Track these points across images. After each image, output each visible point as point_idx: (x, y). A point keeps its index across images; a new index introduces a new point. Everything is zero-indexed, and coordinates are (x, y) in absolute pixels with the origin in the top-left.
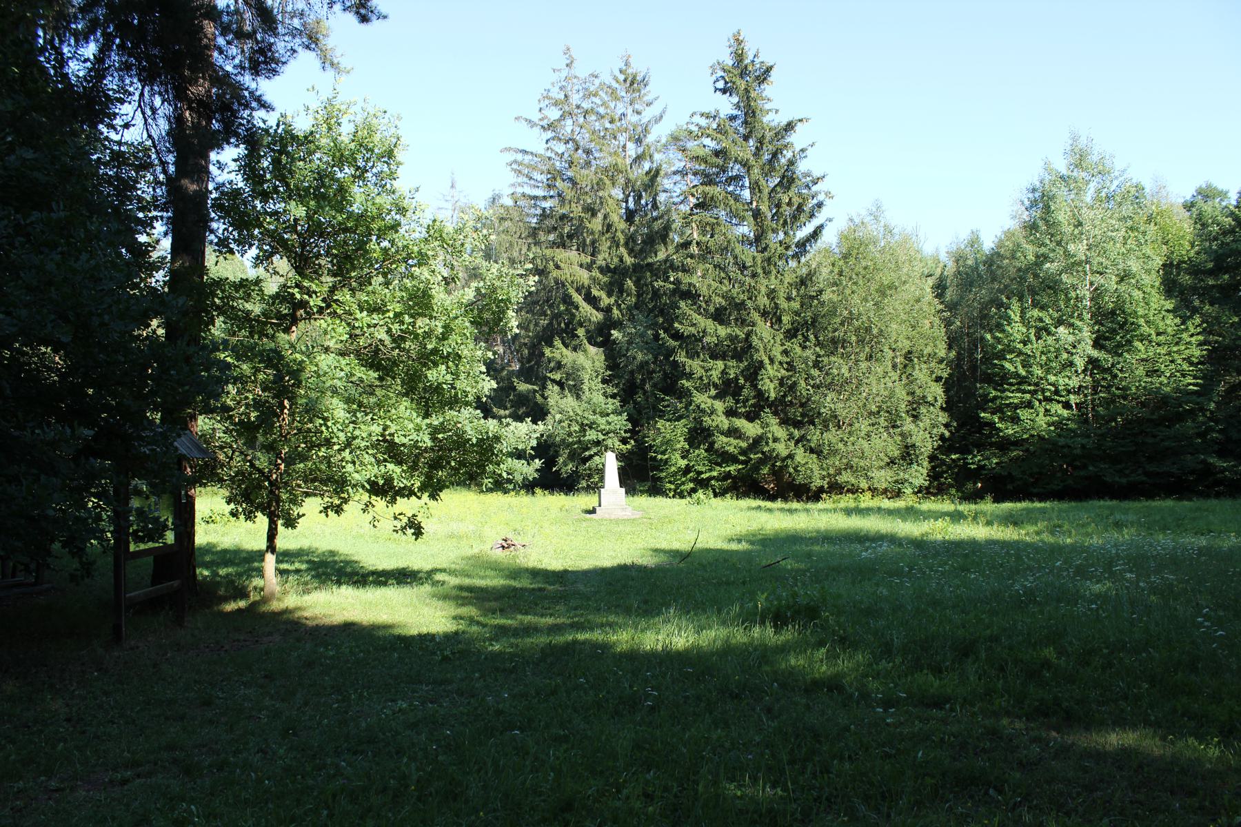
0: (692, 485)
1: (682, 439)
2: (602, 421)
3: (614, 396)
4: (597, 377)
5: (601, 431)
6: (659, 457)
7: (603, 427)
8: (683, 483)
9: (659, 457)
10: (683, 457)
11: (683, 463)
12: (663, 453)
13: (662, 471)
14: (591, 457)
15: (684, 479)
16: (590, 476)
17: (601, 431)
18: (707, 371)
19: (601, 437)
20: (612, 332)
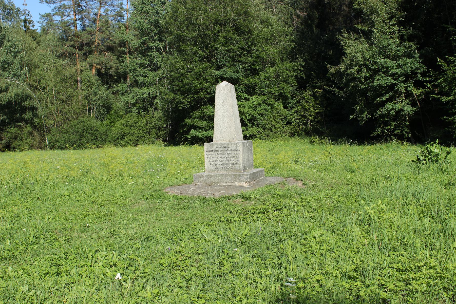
2: (390, 63)
4: (391, 18)
5: (393, 75)
7: (393, 71)
14: (383, 104)
16: (386, 124)
17: (393, 75)
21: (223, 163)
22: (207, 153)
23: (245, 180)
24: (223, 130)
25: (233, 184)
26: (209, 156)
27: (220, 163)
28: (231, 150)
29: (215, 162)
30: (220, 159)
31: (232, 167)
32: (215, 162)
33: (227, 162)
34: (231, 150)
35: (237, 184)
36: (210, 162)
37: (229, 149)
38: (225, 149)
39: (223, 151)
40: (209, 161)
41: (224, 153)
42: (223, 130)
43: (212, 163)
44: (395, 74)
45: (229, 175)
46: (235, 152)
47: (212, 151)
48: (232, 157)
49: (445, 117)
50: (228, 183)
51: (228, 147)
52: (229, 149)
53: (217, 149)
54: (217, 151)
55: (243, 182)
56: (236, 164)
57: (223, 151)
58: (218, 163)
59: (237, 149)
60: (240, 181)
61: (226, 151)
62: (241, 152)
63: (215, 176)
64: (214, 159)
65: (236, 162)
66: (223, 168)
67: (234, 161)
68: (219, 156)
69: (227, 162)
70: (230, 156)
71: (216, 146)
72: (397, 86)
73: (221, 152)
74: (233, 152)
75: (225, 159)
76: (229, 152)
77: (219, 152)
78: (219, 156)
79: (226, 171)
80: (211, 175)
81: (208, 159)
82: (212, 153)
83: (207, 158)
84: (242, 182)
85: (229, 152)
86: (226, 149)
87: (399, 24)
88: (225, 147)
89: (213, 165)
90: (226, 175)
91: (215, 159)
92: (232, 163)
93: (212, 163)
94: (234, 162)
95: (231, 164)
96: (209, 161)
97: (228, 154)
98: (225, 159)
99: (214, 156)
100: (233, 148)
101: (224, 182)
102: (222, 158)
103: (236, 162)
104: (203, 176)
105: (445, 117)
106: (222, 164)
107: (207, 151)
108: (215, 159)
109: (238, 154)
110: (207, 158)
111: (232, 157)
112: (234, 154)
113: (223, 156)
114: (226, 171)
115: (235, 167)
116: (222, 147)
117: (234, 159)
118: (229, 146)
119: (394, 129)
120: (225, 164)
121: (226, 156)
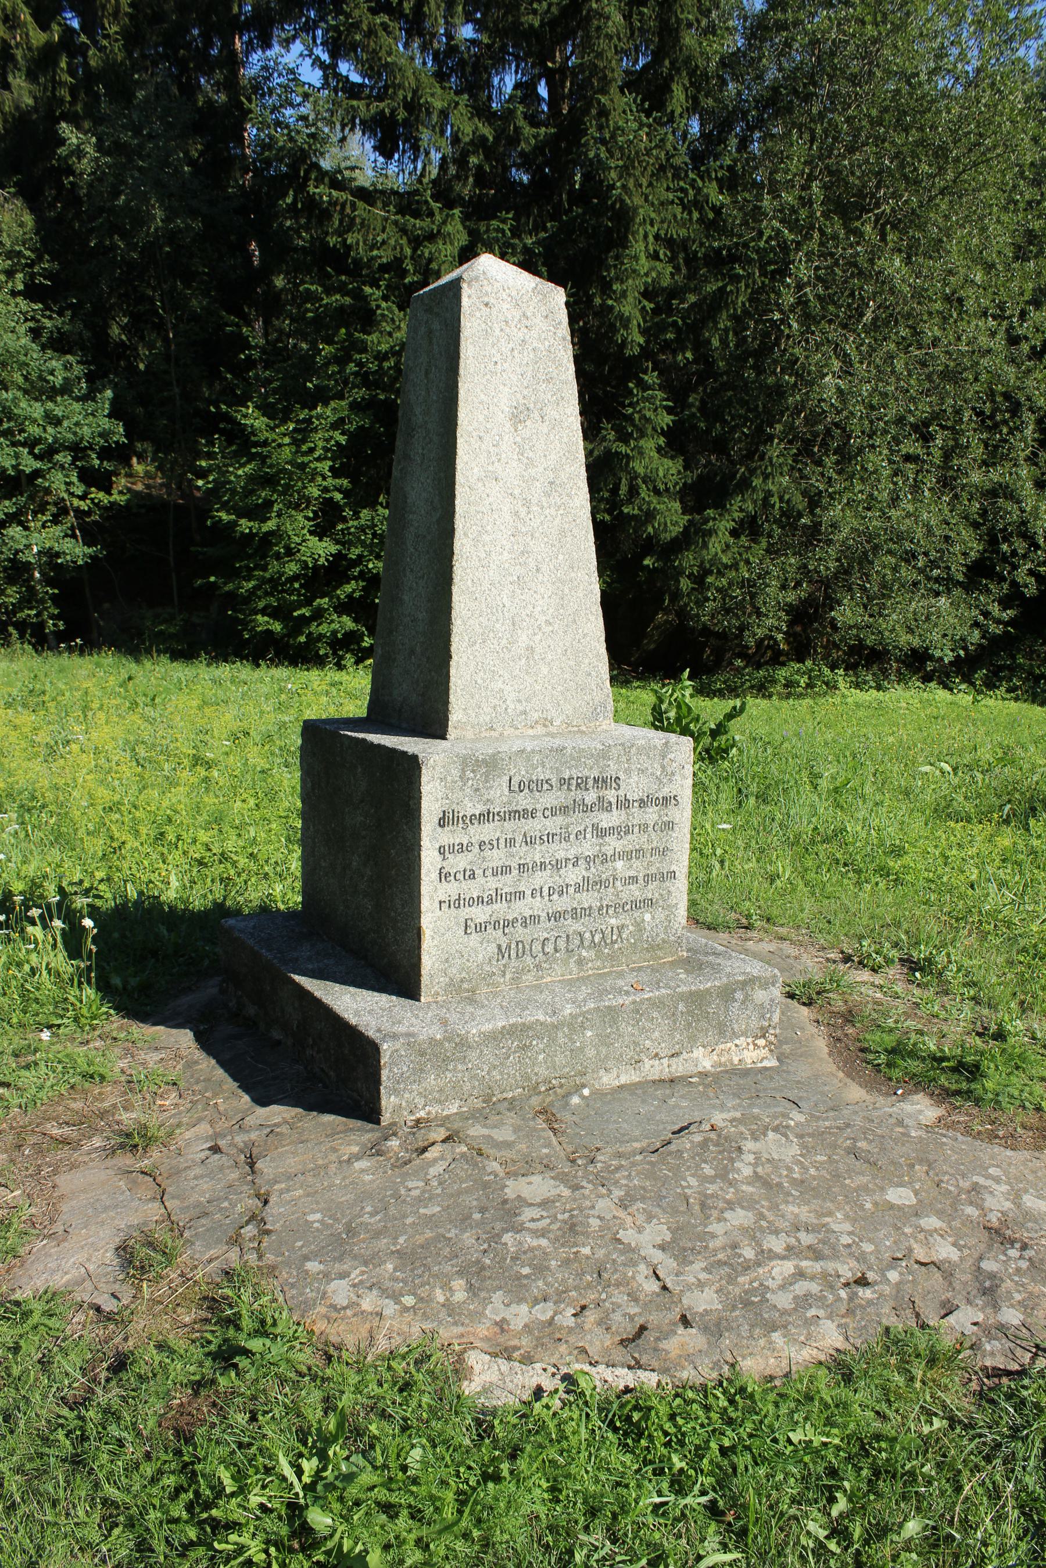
0: (348, 623)
1: (325, 466)
3: (59, 344)
5: (31, 444)
6: (245, 525)
7: (34, 430)
8: (318, 615)
9: (245, 525)
10: (320, 532)
11: (322, 549)
12: (258, 514)
13: (234, 574)
15: (324, 602)
17: (31, 444)
18: (416, 242)
19: (30, 464)
20: (65, 129)
21: (562, 903)
22: (448, 837)
23: (755, 1024)
24: (523, 640)
25: (678, 1068)
26: (458, 862)
27: (536, 906)
28: (624, 804)
29: (500, 909)
30: (542, 879)
31: (621, 928)
32: (500, 909)
33: (588, 899)
34: (624, 804)
35: (703, 1059)
36: (466, 912)
37: (611, 795)
38: (579, 795)
39: (564, 810)
40: (458, 903)
41: (574, 829)
42: (523, 640)
43: (480, 914)
44: (38, 441)
45: (657, 1004)
46: (651, 814)
47: (485, 817)
48: (627, 855)
49: (212, 579)
50: (648, 1063)
51: (601, 782)
52: (611, 795)
53: (524, 801)
54: (528, 814)
55: (745, 1034)
56: (649, 903)
57: (564, 810)
58: (522, 908)
59: (665, 791)
60: (724, 1031)
61: (588, 809)
62: (683, 815)
63: (556, 1027)
64: (493, 883)
65: (652, 890)
66: (562, 944)
67: (634, 880)
68: (537, 853)
69: (588, 899)
70: (613, 844)
71: (520, 772)
72: (44, 477)
73: (553, 824)
74: (637, 816)
75: (573, 875)
76: (606, 820)
77: (535, 826)
78: (537, 853)
79: (580, 962)
80: (525, 1028)
81: (451, 889)
82: (487, 831)
83: (443, 876)
84: (735, 1035)
85: (606, 820)
86: (591, 797)
87: (31, 292)
88: (582, 784)
89: (481, 928)
90: (637, 1010)
91: (506, 883)
92: (625, 896)
93: (480, 914)
94: (635, 891)
95: (620, 907)
96: (458, 903)
97: (601, 833)
98: (573, 875)
99: (497, 857)
100: (634, 787)
101: (619, 1060)
102: (557, 865)
103: (652, 890)
104: (463, 1044)
105: (212, 579)
106: (556, 916)
107: (442, 823)
108: (506, 883)
109: (669, 826)
110: (443, 876)
111: (627, 855)
112: (644, 828)
113: (561, 855)
114: (580, 962)
115: (639, 925)
116: (562, 781)
117: (638, 868)
118: (612, 770)
119: (18, 607)
120: (575, 914)
121: (588, 847)
